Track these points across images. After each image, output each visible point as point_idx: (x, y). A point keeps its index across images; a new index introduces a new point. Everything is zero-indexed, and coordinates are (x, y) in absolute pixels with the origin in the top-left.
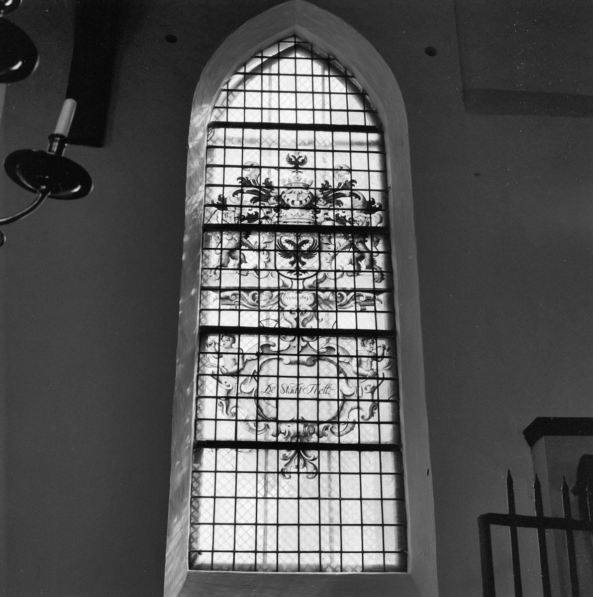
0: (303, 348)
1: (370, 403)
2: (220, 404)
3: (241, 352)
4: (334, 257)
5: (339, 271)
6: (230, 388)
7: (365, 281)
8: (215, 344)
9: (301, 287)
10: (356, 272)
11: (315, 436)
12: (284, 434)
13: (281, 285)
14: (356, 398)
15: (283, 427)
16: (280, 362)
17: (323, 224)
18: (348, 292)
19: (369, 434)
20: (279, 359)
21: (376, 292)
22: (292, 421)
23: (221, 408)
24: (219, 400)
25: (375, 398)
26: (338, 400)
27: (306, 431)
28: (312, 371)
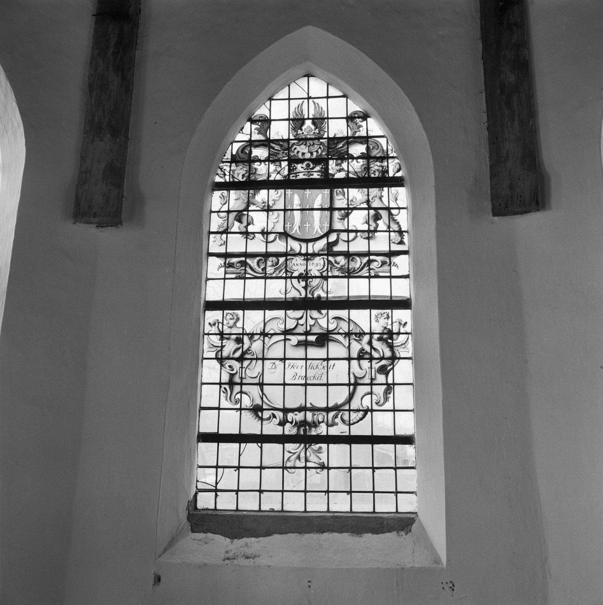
0: (311, 326)
1: (385, 386)
2: (224, 390)
3: (245, 332)
4: (347, 215)
5: (352, 231)
6: (234, 372)
7: (381, 243)
8: (218, 323)
9: (310, 251)
10: (370, 234)
11: (323, 426)
12: (291, 423)
13: (288, 250)
14: (368, 381)
15: (290, 416)
16: (287, 342)
17: (336, 177)
18: (361, 255)
19: (383, 424)
20: (285, 340)
21: (391, 254)
22: (300, 409)
23: (225, 395)
24: (223, 386)
25: (390, 381)
26: (349, 385)
27: (315, 420)
28: (320, 353)
